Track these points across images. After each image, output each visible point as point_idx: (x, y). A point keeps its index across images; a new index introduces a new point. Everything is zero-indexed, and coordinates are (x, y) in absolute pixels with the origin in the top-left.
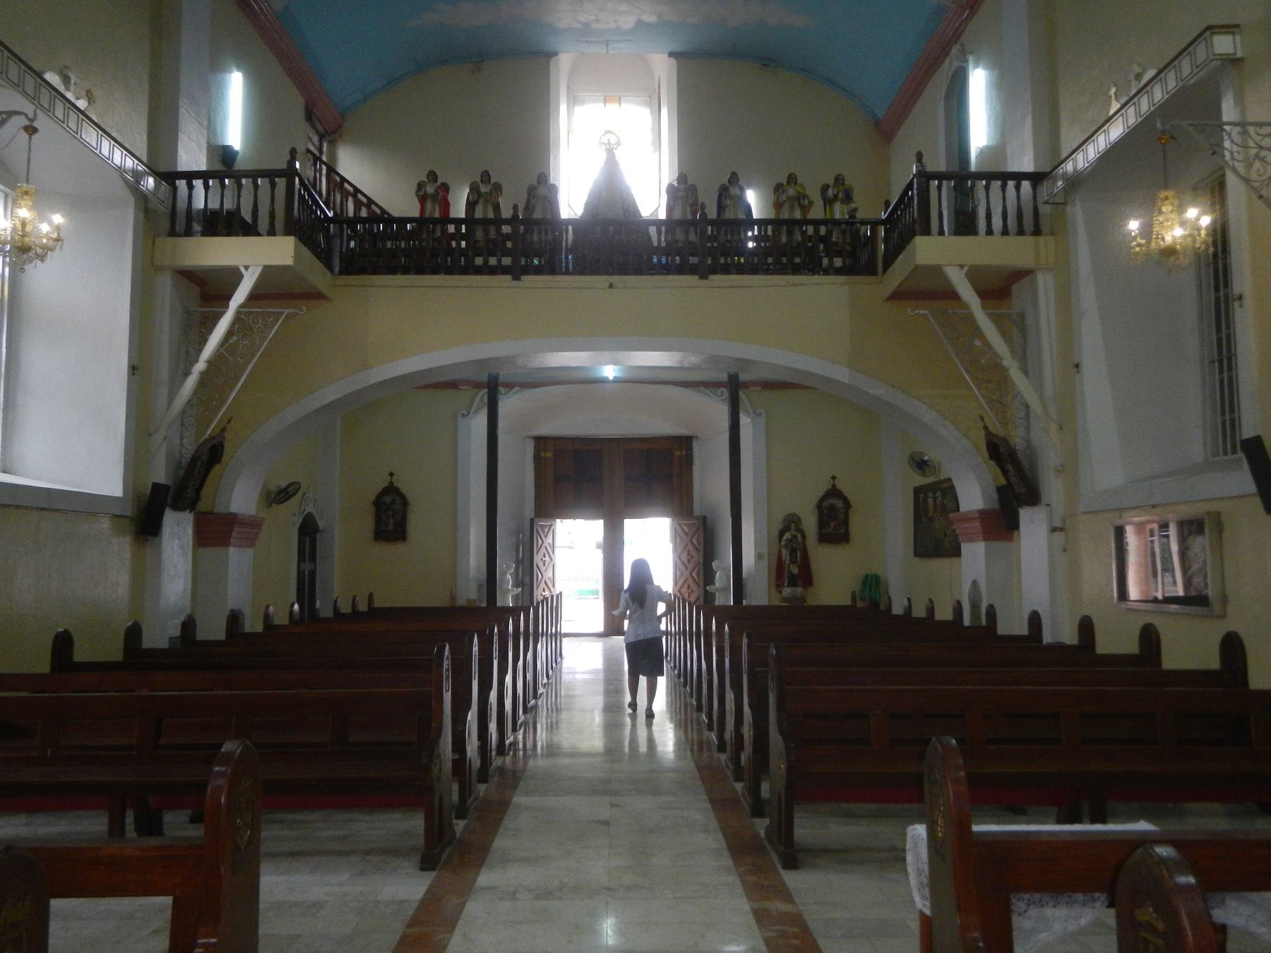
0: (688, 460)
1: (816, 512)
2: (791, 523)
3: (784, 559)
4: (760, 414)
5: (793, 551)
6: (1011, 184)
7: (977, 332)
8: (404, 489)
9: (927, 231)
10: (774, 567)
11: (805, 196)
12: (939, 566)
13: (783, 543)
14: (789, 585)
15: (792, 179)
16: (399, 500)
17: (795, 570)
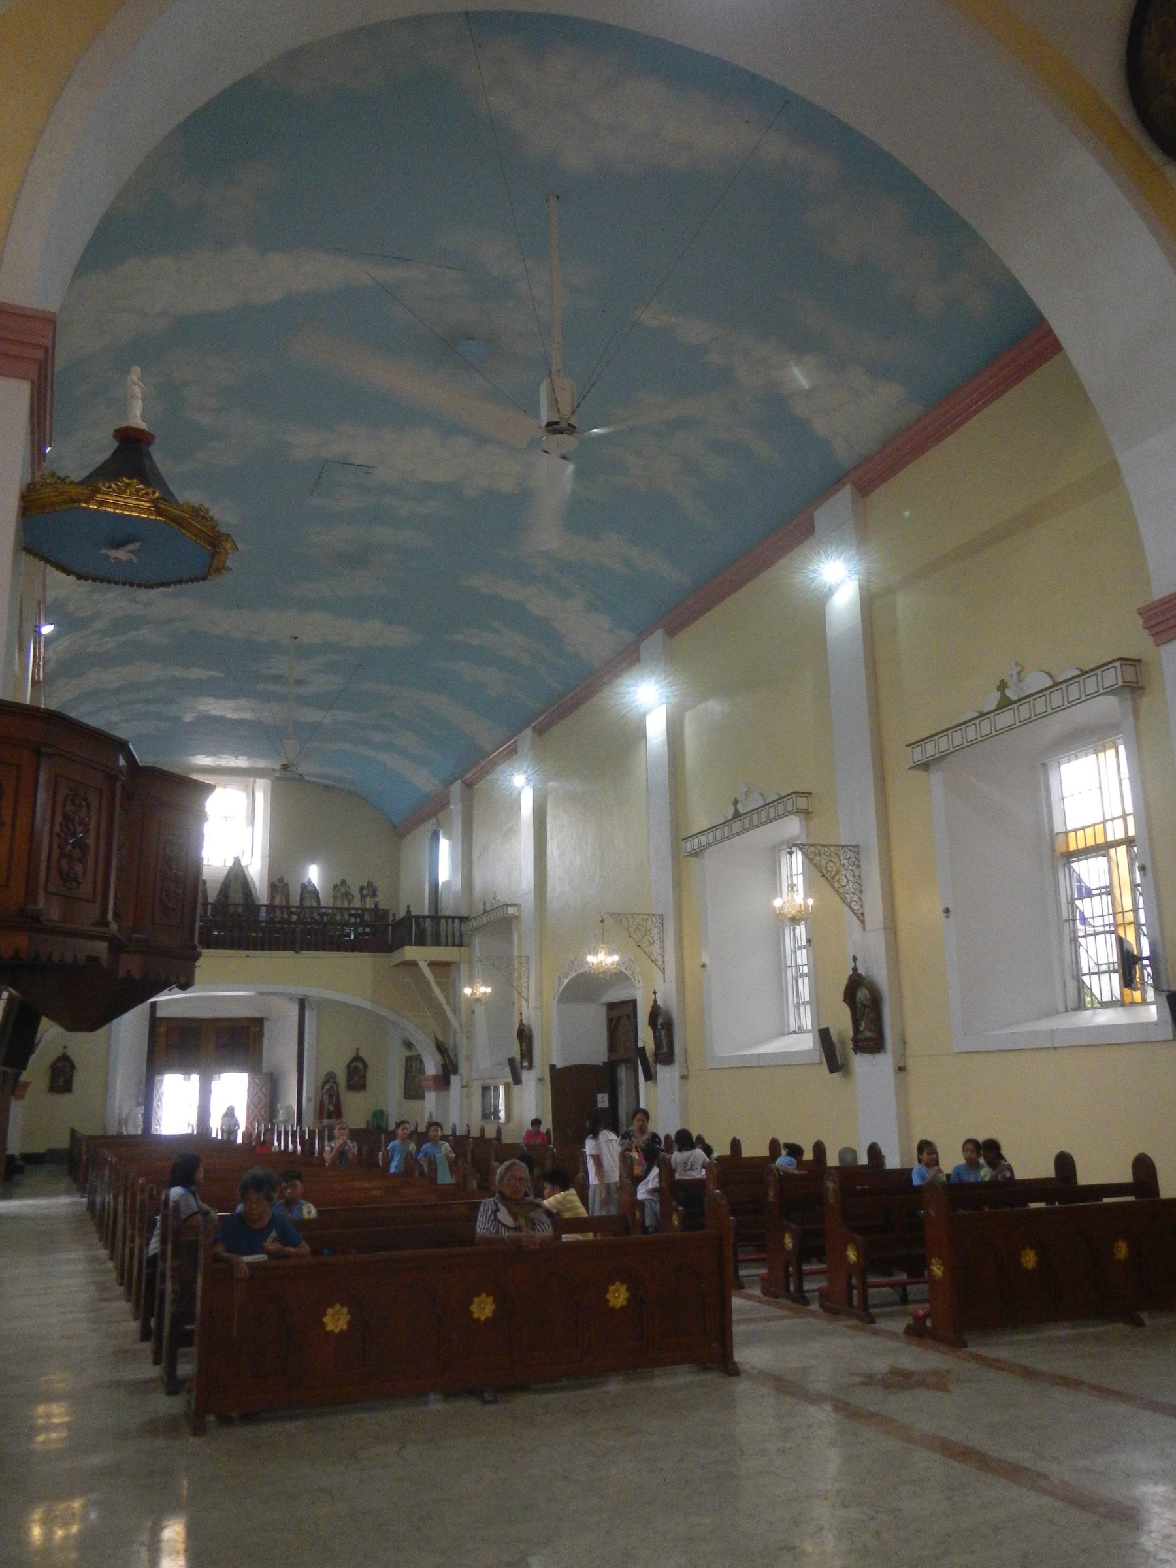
0: (260, 1035)
1: (346, 1071)
2: (331, 1078)
3: (324, 1100)
4: (314, 1008)
5: (331, 1096)
6: (450, 920)
7: (431, 990)
8: (72, 1057)
9: (410, 944)
10: (318, 1107)
11: (350, 894)
12: (415, 1104)
13: (324, 1091)
14: (327, 1118)
15: (343, 883)
16: (68, 1065)
17: (331, 1108)
